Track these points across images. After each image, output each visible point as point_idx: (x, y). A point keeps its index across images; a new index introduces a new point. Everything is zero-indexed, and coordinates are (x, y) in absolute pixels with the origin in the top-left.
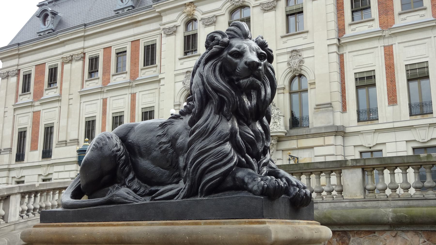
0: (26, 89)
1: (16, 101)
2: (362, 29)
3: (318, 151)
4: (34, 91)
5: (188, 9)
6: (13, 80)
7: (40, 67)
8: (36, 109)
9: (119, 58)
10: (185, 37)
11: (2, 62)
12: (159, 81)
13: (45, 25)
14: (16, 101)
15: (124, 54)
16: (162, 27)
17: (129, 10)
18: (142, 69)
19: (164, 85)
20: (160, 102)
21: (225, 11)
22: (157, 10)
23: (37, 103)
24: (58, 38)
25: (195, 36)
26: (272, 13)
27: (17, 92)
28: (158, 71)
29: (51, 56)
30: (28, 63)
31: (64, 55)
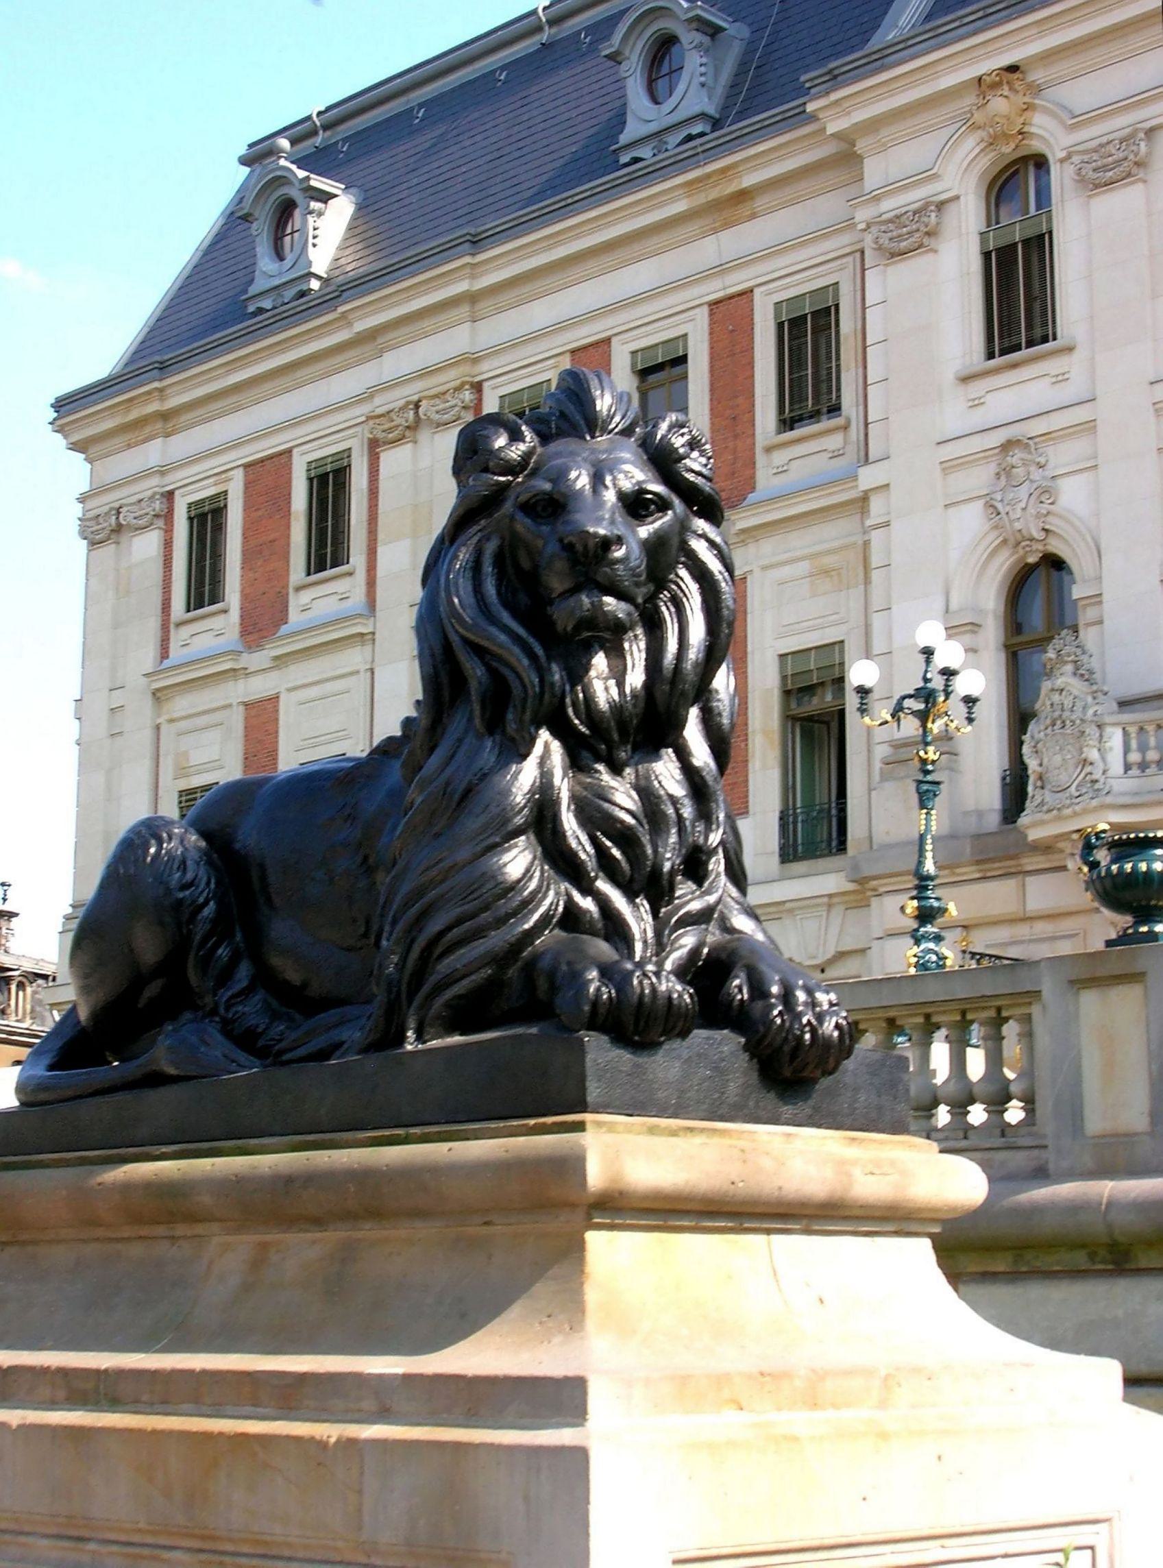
0: (204, 589)
1: (164, 653)
4: (245, 596)
5: (999, 105)
6: (147, 545)
7: (266, 476)
8: (258, 687)
9: (652, 395)
10: (987, 256)
11: (89, 460)
12: (865, 498)
13: (280, 256)
14: (164, 653)
15: (678, 370)
16: (863, 215)
17: (690, 138)
18: (769, 450)
19: (887, 524)
20: (877, 621)
22: (831, 129)
25: (1039, 246)
28: (852, 454)
31: (381, 403)
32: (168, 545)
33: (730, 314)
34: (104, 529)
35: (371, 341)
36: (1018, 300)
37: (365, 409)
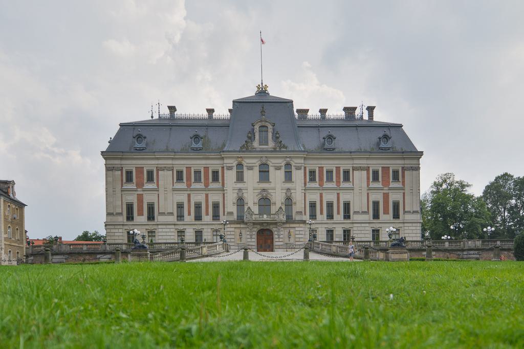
1: (122, 186)
2: (313, 185)
3: (297, 229)
12: (224, 190)
14: (122, 186)
21: (257, 164)
22: (223, 156)
23: (139, 190)
24: (155, 155)
26: (279, 171)
27: (122, 180)
29: (149, 164)
30: (131, 164)
31: (159, 166)
32: (122, 173)
33: (206, 169)
34: (109, 169)
35: (158, 159)
36: (240, 178)
37: (157, 166)
